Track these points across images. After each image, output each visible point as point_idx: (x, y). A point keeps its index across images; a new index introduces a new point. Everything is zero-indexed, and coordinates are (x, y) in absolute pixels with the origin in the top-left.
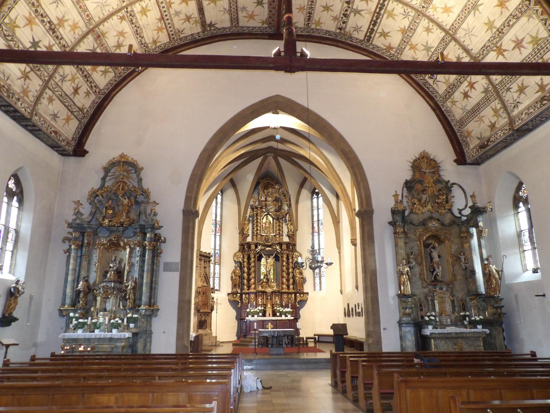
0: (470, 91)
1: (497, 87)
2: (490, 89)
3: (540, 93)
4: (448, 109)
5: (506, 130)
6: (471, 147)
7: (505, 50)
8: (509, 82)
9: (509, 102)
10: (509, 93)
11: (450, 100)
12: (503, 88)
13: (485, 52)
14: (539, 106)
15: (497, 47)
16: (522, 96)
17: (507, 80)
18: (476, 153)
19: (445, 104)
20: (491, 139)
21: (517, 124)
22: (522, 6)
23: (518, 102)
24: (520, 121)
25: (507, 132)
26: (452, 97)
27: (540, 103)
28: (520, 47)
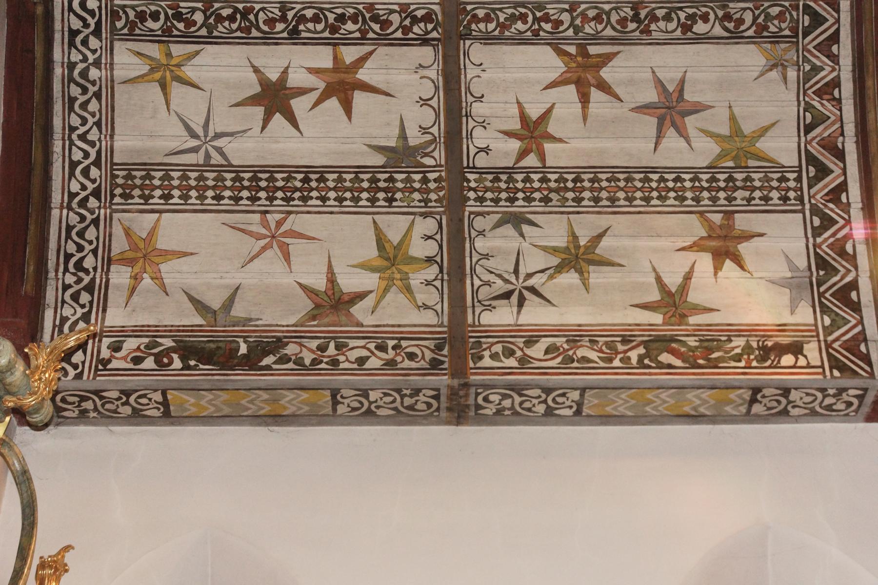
0: (314, 96)
1: (471, 177)
2: (428, 161)
3: (657, 318)
4: (94, 73)
5: (412, 356)
6: (115, 317)
7: (604, 87)
8: (537, 195)
9: (490, 264)
10: (508, 230)
11: (154, 50)
12: (496, 201)
13: (520, 25)
14: (634, 355)
15: (586, 55)
16: (570, 278)
17: (536, 185)
18: (137, 360)
19: (93, 42)
20: (291, 349)
21: (487, 362)
22: (781, 13)
23: (533, 290)
24: (512, 362)
25: (407, 363)
26: (177, 50)
27: (642, 350)
28: (668, 122)
